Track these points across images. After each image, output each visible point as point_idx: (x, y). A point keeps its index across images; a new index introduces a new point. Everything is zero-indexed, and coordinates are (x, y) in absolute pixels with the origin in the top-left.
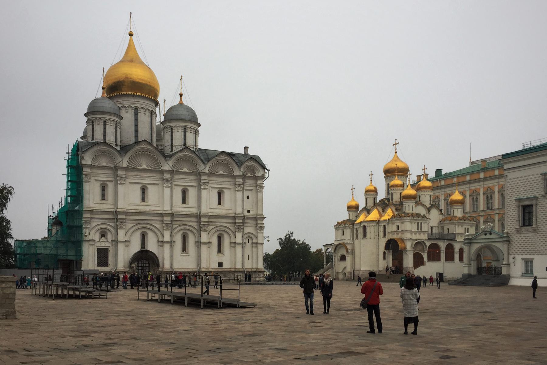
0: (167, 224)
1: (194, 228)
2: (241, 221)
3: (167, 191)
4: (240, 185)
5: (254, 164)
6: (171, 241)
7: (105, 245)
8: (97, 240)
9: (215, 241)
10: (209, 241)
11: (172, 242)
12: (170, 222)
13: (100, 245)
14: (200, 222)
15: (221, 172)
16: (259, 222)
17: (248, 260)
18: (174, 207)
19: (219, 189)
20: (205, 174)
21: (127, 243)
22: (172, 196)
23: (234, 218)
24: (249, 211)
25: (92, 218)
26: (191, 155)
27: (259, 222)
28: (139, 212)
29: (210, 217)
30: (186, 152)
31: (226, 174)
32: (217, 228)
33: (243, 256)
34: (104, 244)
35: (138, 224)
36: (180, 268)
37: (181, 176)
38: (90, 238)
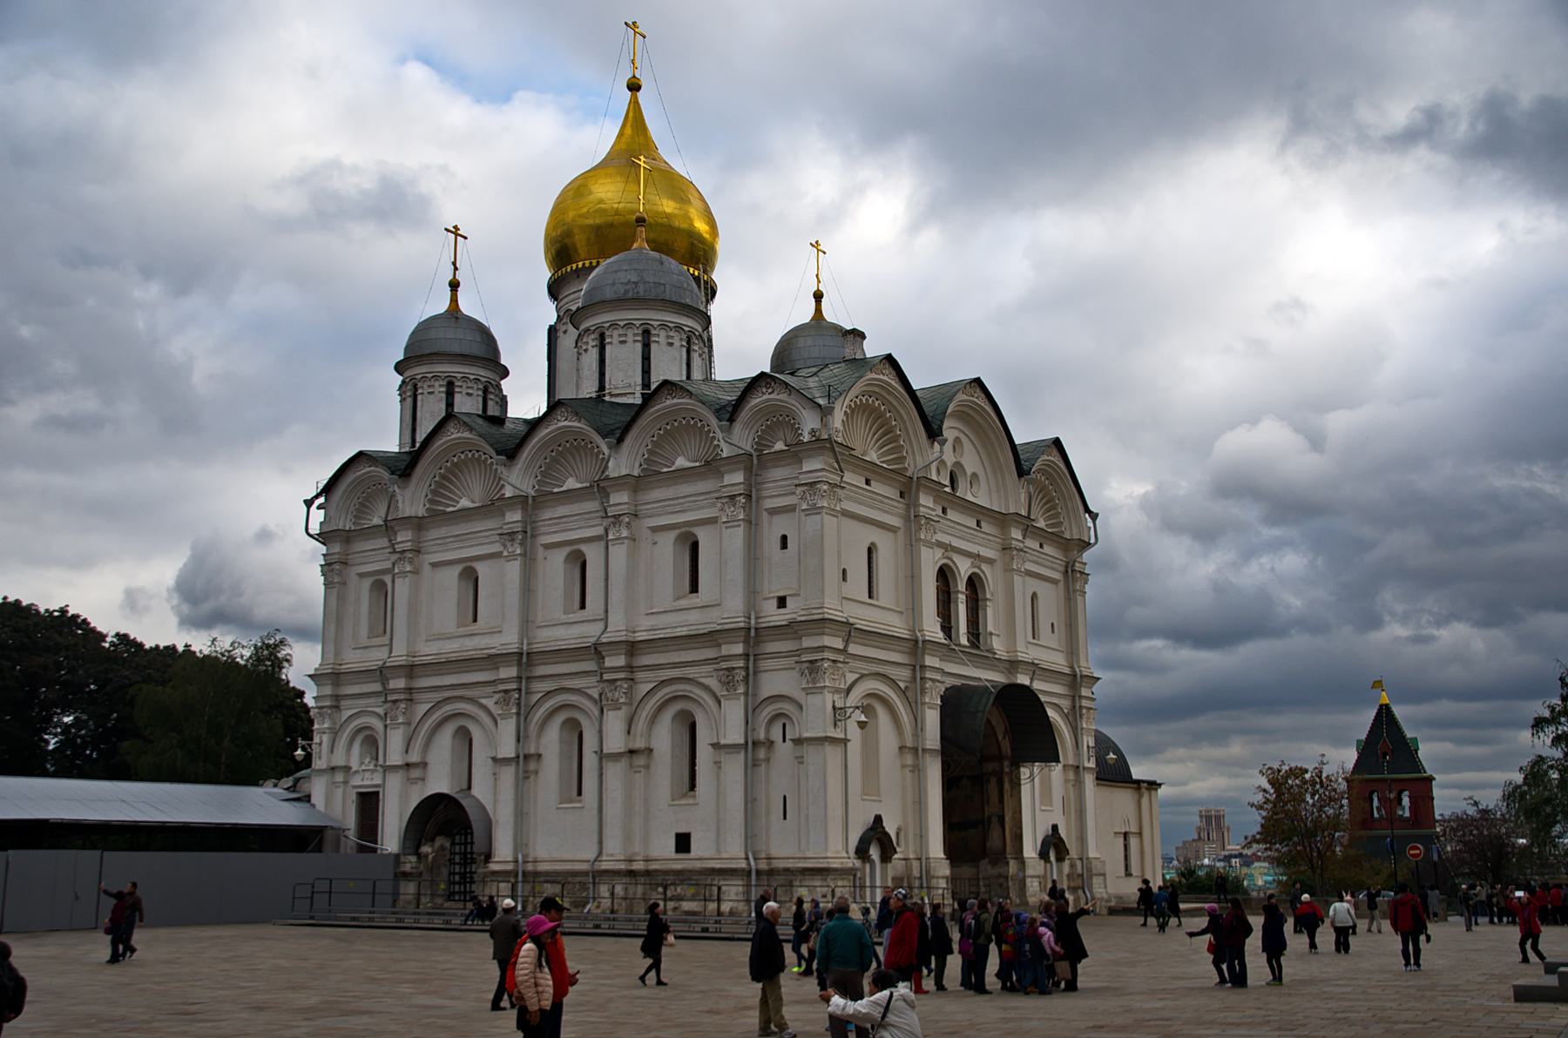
0: (506, 691)
1: (590, 697)
2: (739, 649)
3: (514, 569)
4: (732, 497)
5: (780, 397)
6: (518, 757)
7: (374, 782)
9: (664, 738)
12: (514, 686)
13: (360, 783)
15: (681, 462)
17: (785, 818)
18: (538, 627)
19: (678, 531)
20: (622, 482)
21: (416, 773)
23: (712, 638)
24: (782, 602)
26: (576, 424)
27: (807, 642)
28: (443, 660)
29: (632, 648)
30: (559, 418)
31: (697, 464)
33: (750, 802)
34: (367, 780)
35: (447, 700)
36: (557, 856)
37: (562, 510)
38: (342, 763)
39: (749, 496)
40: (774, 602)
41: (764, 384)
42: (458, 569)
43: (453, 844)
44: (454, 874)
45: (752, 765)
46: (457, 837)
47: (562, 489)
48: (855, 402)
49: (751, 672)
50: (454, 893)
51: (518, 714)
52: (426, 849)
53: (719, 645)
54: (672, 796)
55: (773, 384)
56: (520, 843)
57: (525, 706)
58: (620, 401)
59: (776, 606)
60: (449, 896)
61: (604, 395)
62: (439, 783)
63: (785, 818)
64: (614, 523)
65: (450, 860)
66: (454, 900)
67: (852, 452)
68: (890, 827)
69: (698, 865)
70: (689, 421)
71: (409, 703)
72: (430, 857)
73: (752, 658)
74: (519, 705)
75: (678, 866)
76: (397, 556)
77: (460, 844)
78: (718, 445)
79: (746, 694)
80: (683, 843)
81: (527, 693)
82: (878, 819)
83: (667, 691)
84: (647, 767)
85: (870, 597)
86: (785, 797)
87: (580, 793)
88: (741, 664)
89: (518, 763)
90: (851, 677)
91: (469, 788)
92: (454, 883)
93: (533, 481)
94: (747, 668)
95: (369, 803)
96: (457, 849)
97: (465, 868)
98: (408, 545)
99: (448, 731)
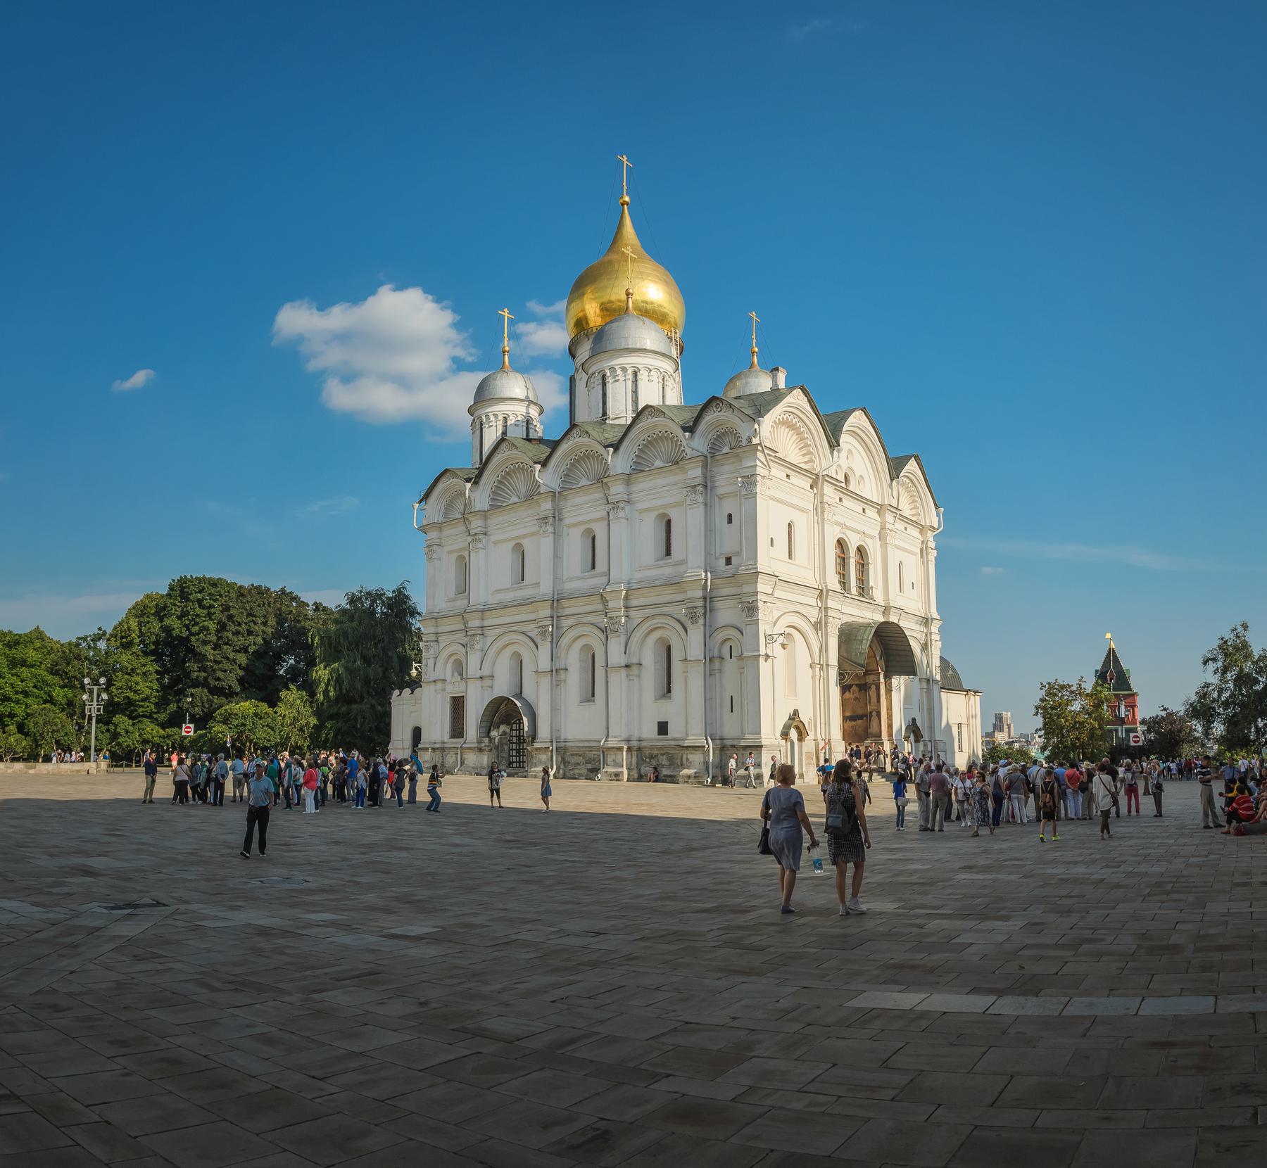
3: (547, 543)
8: (448, 678)
10: (631, 662)
11: (554, 671)
14: (606, 613)
16: (747, 589)
17: (732, 711)
19: (656, 513)
21: (487, 682)
22: (557, 556)
24: (729, 561)
25: (438, 635)
32: (650, 623)
33: (708, 700)
36: (578, 737)
38: (438, 674)
39: (705, 486)
40: (723, 562)
41: (714, 405)
42: (511, 544)
43: (512, 730)
44: (512, 749)
45: (710, 674)
46: (514, 725)
47: (578, 486)
48: (779, 419)
49: (708, 609)
50: (513, 762)
51: (552, 642)
52: (494, 733)
53: (686, 592)
54: (655, 696)
55: (721, 404)
56: (554, 729)
57: (556, 636)
58: (617, 423)
59: (724, 564)
60: (509, 765)
61: (606, 419)
62: (502, 688)
63: (732, 711)
64: (613, 508)
65: (509, 741)
66: (513, 767)
67: (777, 455)
68: (805, 717)
69: (673, 743)
70: (663, 433)
71: (481, 636)
72: (497, 740)
73: (708, 600)
74: (552, 635)
75: (660, 744)
76: (470, 539)
77: (516, 730)
78: (684, 450)
79: (705, 625)
80: (663, 728)
81: (557, 628)
82: (796, 712)
83: (650, 623)
84: (639, 676)
85: (790, 558)
86: (732, 697)
87: (593, 696)
88: (701, 604)
89: (552, 675)
90: (776, 614)
91: (521, 693)
92: (513, 756)
93: (559, 481)
94: (705, 607)
95: (458, 705)
96: (514, 732)
97: (519, 746)
98: (477, 531)
99: (508, 652)
